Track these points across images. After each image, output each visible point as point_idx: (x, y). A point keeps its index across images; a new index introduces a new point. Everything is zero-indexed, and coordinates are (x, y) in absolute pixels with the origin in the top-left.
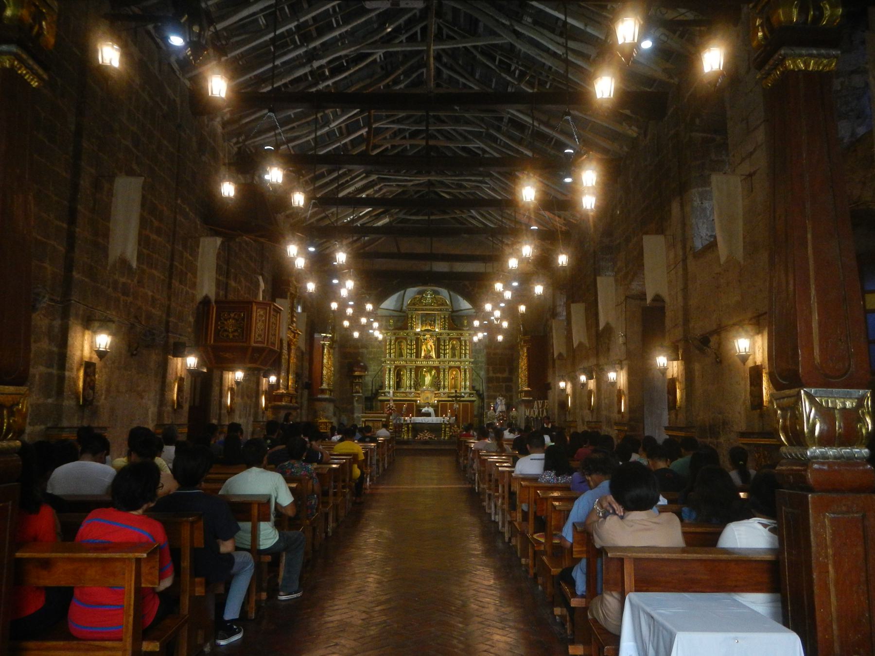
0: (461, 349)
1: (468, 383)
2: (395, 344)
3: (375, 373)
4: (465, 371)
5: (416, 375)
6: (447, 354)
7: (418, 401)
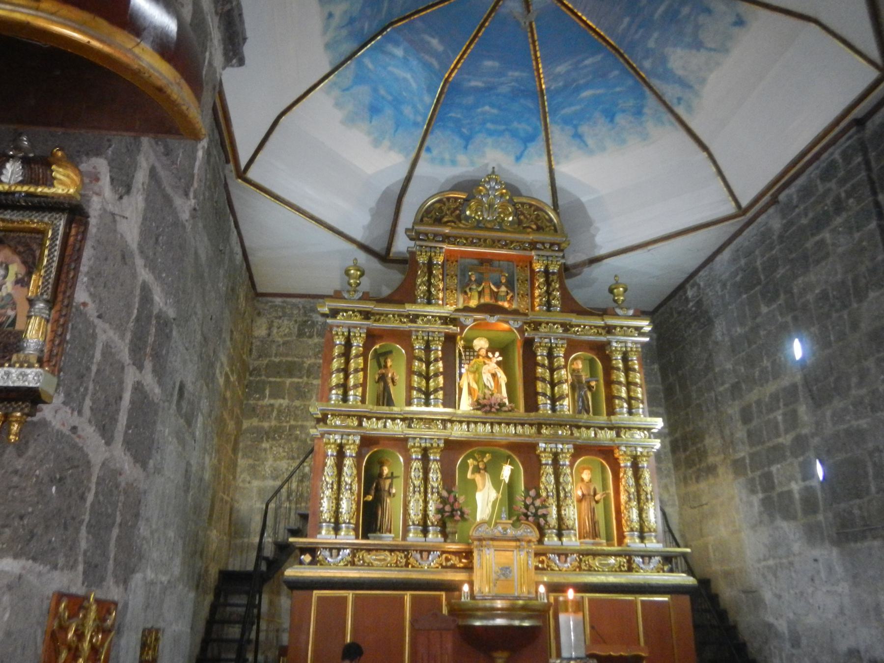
0: (609, 383)
1: (653, 515)
3: (278, 483)
6: (562, 398)
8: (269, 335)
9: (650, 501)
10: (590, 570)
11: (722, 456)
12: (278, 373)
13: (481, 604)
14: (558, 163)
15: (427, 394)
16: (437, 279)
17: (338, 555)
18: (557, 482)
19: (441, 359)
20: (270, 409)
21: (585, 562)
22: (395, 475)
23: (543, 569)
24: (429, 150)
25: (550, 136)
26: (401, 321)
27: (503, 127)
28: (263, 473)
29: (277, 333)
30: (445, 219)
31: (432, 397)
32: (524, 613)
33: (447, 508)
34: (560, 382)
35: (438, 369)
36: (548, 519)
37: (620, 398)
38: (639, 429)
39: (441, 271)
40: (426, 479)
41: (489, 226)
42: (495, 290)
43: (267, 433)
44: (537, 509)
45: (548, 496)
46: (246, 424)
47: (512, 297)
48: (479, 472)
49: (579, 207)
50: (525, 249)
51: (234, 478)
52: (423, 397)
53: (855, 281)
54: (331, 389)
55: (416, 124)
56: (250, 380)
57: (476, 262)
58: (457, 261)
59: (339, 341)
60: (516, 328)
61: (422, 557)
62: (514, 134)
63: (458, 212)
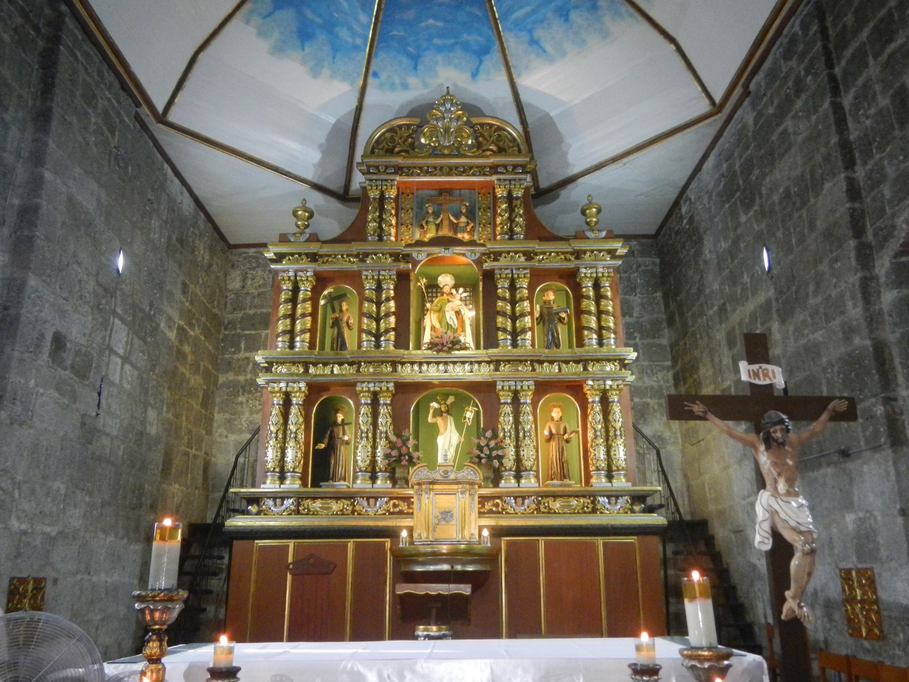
0: (579, 312)
1: (620, 453)
2: (314, 300)
4: (605, 401)
5: (399, 422)
6: (524, 331)
7: (404, 534)
8: (243, 287)
9: (619, 438)
10: (550, 512)
11: (713, 386)
12: (253, 325)
13: (422, 549)
14: (519, 76)
15: (377, 336)
16: (388, 214)
17: (282, 504)
18: (517, 422)
19: (393, 298)
20: (245, 362)
21: (544, 504)
22: (346, 422)
23: (499, 513)
24: (375, 75)
25: (505, 45)
26: (350, 261)
27: (452, 41)
28: (240, 426)
29: (251, 284)
30: (397, 150)
31: (382, 338)
32: (469, 558)
33: (395, 453)
34: (523, 315)
35: (390, 307)
36: (504, 461)
37: (589, 329)
38: (609, 360)
39: (393, 205)
40: (375, 424)
41: (446, 152)
42: (455, 221)
43: (242, 387)
44: (491, 450)
45: (505, 437)
46: (222, 379)
47: (473, 227)
48: (442, 416)
49: (548, 122)
50: (484, 175)
51: (209, 432)
52: (373, 339)
53: (812, 172)
54: (278, 336)
55: (355, 48)
56: (225, 335)
57: (434, 192)
58: (413, 194)
59: (287, 286)
60: (473, 261)
61: (369, 504)
62: (466, 47)
63: (410, 140)
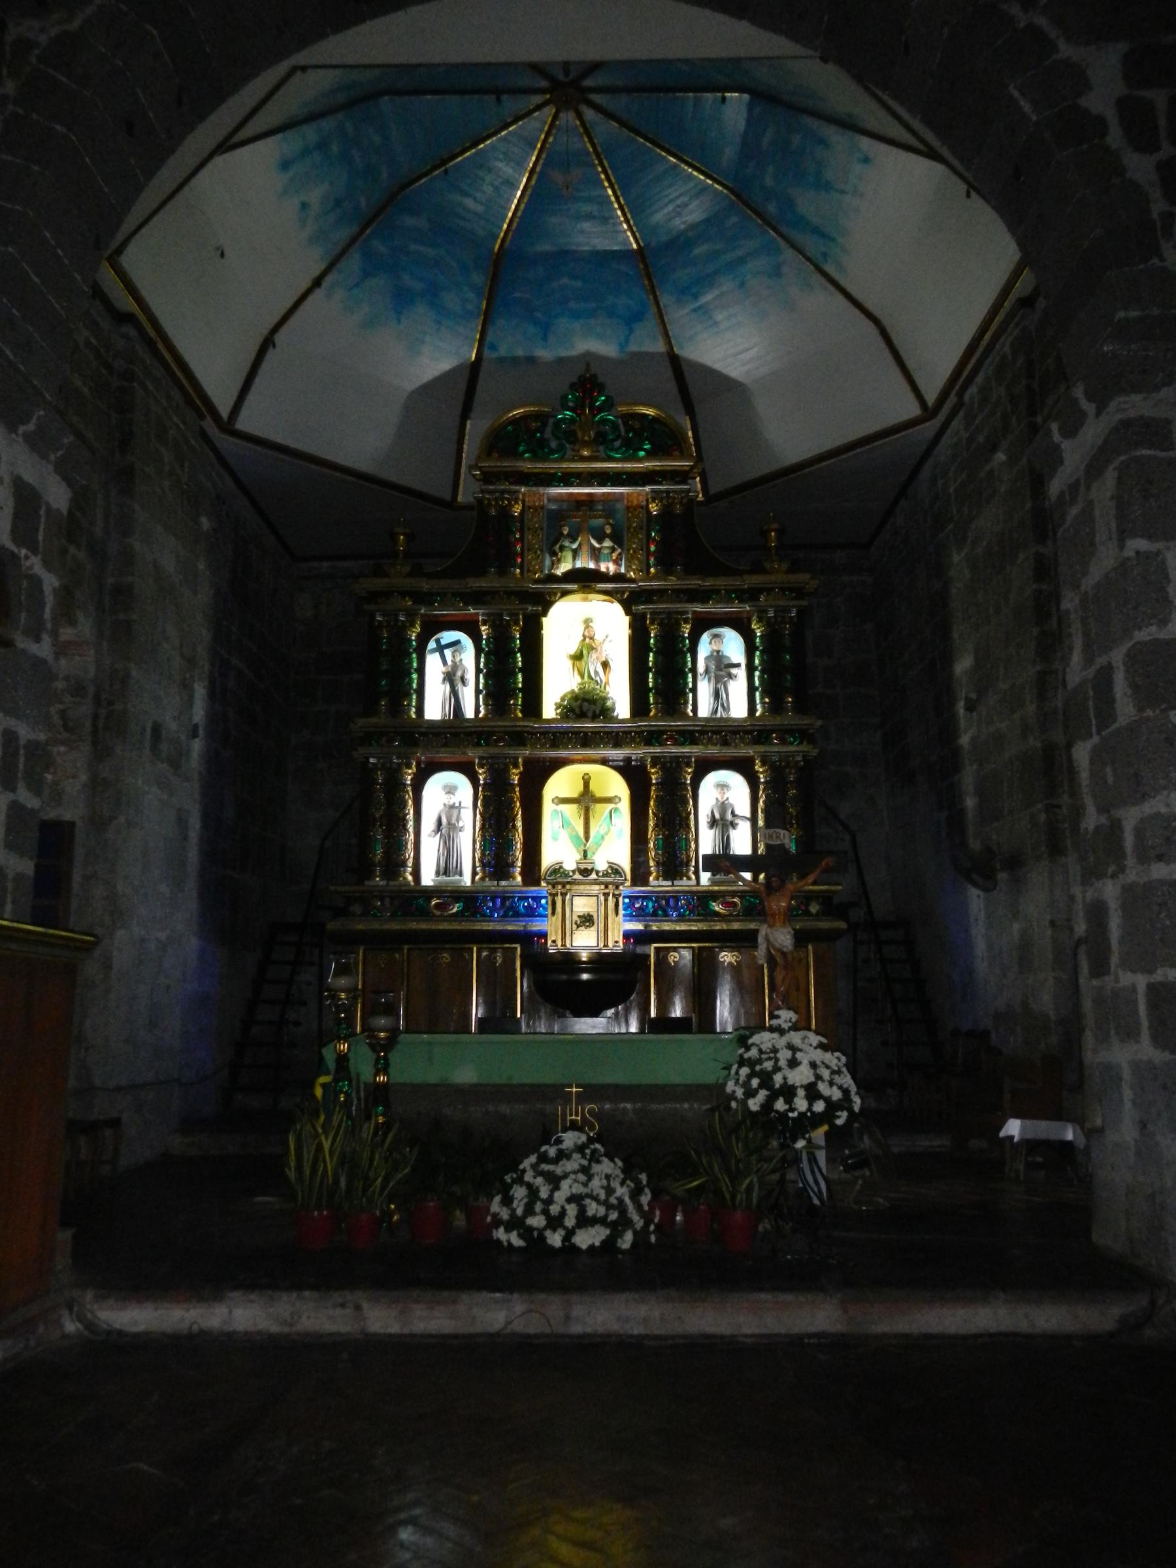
14: (682, 348)
24: (493, 347)
25: (664, 312)
27: (594, 305)
42: (597, 545)
47: (620, 554)
62: (611, 313)
